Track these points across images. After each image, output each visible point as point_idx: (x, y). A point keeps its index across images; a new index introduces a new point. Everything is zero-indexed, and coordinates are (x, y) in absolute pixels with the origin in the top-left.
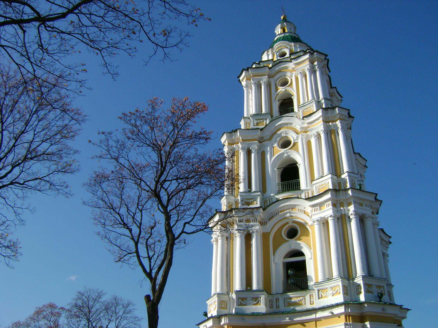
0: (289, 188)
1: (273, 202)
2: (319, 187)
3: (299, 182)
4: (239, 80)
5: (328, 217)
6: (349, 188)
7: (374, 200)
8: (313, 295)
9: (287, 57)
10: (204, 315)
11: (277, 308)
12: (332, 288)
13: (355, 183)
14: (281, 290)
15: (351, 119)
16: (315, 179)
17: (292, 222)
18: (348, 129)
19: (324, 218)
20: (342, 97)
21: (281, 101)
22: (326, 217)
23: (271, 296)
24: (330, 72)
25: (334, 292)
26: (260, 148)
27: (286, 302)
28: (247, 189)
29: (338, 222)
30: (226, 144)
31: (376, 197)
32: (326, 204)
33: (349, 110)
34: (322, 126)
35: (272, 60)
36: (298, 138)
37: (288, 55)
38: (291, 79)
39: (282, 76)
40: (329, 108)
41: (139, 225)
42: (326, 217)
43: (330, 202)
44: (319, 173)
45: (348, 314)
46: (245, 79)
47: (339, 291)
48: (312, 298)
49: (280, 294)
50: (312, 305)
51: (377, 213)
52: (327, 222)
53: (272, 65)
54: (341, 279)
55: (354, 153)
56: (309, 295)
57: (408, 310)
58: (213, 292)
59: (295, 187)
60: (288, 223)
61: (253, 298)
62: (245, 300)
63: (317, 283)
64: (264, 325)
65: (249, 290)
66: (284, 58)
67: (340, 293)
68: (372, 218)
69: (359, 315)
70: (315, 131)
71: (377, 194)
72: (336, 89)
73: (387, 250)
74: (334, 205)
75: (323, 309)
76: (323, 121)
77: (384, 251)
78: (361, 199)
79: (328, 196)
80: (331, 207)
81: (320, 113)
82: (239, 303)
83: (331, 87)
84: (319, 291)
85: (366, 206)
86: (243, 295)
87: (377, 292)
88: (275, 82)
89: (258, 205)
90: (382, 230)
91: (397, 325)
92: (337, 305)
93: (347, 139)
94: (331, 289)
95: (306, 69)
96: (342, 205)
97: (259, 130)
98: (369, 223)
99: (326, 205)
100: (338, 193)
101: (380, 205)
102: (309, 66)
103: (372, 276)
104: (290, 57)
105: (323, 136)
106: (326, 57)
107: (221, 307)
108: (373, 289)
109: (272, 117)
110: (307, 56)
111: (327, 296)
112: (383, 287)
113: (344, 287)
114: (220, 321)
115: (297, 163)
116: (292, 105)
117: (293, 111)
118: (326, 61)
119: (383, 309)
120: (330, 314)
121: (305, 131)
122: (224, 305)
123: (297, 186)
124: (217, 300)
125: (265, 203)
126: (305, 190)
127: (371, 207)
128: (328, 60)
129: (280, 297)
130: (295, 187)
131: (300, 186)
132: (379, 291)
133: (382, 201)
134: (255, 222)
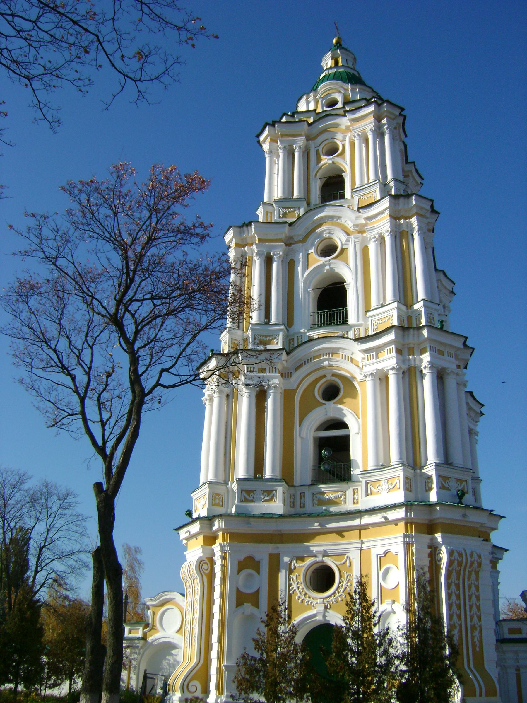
0: (330, 321)
1: (303, 341)
2: (377, 321)
3: (346, 312)
5: (388, 370)
6: (423, 327)
7: (461, 346)
8: (358, 489)
9: (339, 108)
10: (187, 515)
11: (300, 507)
12: (387, 480)
13: (433, 318)
14: (308, 479)
15: (435, 216)
16: (372, 309)
17: (331, 374)
18: (429, 230)
19: (382, 370)
20: (423, 179)
21: (324, 180)
22: (385, 369)
23: (292, 488)
24: (406, 136)
25: (391, 487)
26: (286, 254)
27: (316, 499)
28: (263, 320)
29: (403, 377)
30: (233, 245)
31: (465, 341)
32: (386, 349)
33: (432, 201)
34: (388, 225)
35: (315, 110)
36: (349, 241)
37: (340, 105)
38: (343, 145)
39: (328, 139)
40: (401, 196)
41: (87, 370)
42: (385, 369)
43: (393, 346)
44: (378, 299)
45: (410, 521)
46: (268, 140)
47: (398, 485)
48: (356, 494)
49: (307, 487)
51: (466, 368)
52: (387, 378)
53: (314, 119)
54: (402, 468)
55: (436, 270)
56: (351, 489)
57: (502, 517)
58: (202, 480)
59: (340, 319)
60: (325, 376)
61: (264, 491)
62: (252, 494)
63: (365, 472)
64: (279, 533)
65: (259, 478)
66: (333, 109)
67: (399, 488)
68: (457, 374)
69: (426, 522)
70: (376, 232)
71: (466, 338)
72: (415, 166)
73: (477, 425)
74: (399, 352)
75: (372, 511)
76: (391, 216)
77: (472, 427)
78: (441, 344)
79: (391, 336)
80: (394, 354)
81: (385, 203)
82: (243, 498)
83: (407, 162)
84: (367, 483)
85: (450, 355)
86: (249, 486)
87: (457, 489)
89: (280, 346)
90: (471, 393)
91: (482, 539)
92: (394, 506)
93: (426, 246)
94: (386, 481)
95: (368, 130)
96: (411, 351)
97: (287, 225)
98: (451, 383)
99: (386, 351)
100: (406, 332)
101: (471, 356)
102: (373, 124)
103: (450, 464)
104: (344, 107)
105: (388, 240)
106: (401, 111)
107: (214, 502)
108: (450, 484)
109: (308, 204)
110: (371, 108)
111: (380, 492)
112: (466, 481)
113: (407, 479)
114: (212, 525)
115: (346, 282)
116: (343, 187)
117: (342, 196)
118: (402, 118)
119: (464, 515)
120: (383, 520)
121: (361, 230)
122: (219, 501)
123: (343, 319)
124: (208, 493)
125: (290, 343)
126: (354, 326)
127: (457, 357)
128: (405, 117)
129: (306, 490)
130: (340, 319)
131: (346, 318)
132: (460, 488)
133: (473, 349)
134: (272, 372)
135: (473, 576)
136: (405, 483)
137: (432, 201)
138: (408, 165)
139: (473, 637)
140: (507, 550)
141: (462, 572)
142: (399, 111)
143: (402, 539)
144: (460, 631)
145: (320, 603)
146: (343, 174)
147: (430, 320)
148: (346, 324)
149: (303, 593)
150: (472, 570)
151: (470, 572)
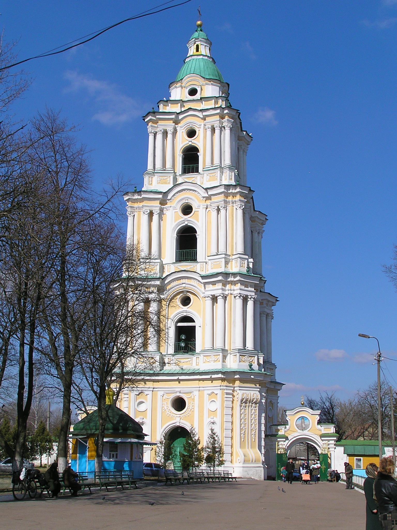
3: (196, 252)
4: (144, 120)
22: (216, 295)
26: (161, 210)
33: (250, 187)
37: (198, 96)
42: (216, 295)
47: (219, 359)
48: (198, 360)
74: (224, 285)
79: (220, 278)
83: (242, 130)
90: (269, 294)
100: (228, 275)
117: (197, 171)
123: (195, 256)
128: (240, 113)
137: (250, 187)
141: (248, 404)
146: (198, 153)
148: (196, 260)
150: (254, 403)
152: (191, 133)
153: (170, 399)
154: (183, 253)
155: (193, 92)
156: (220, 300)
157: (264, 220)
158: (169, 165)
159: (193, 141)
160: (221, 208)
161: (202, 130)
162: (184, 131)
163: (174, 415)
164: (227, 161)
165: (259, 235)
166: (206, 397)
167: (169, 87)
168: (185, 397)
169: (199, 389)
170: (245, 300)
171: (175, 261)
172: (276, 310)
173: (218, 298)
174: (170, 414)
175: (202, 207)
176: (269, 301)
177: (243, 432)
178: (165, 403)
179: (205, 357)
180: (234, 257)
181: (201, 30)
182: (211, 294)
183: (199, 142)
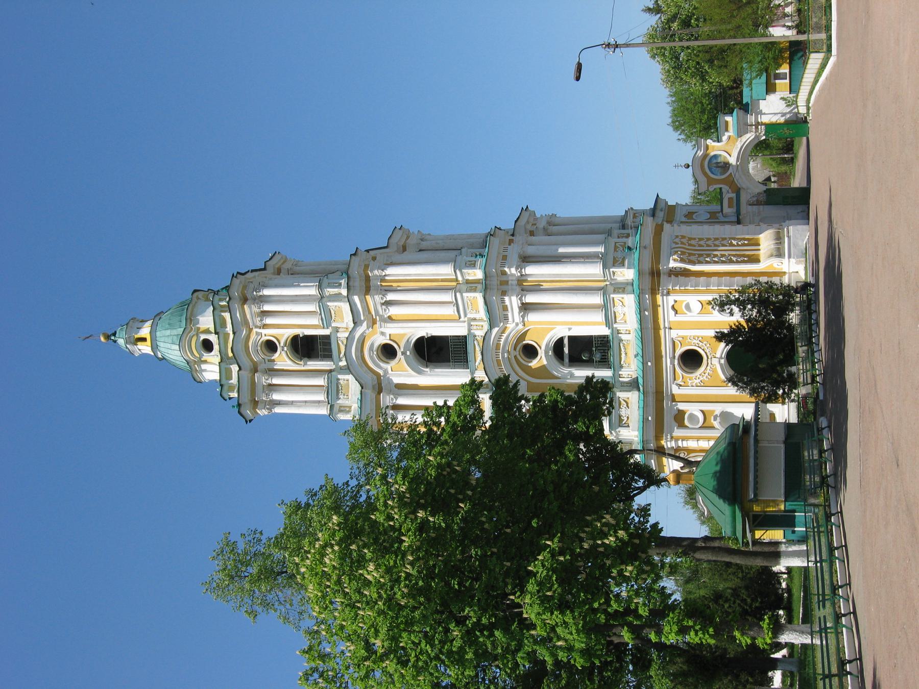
4: (250, 421)
26: (390, 392)
37: (213, 338)
42: (520, 305)
47: (620, 299)
50: (631, 332)
67: (623, 298)
83: (265, 269)
88: (267, 361)
90: (516, 222)
100: (488, 286)
112: (616, 243)
117: (328, 337)
118: (239, 275)
123: (459, 339)
126: (469, 330)
128: (238, 273)
131: (459, 336)
135: (693, 242)
136: (619, 293)
137: (351, 255)
138: (268, 268)
139: (738, 245)
140: (658, 195)
142: (234, 278)
143: (665, 297)
144: (734, 256)
145: (711, 361)
146: (301, 336)
147: (472, 264)
148: (466, 337)
149: (703, 374)
151: (690, 245)
152: (271, 346)
153: (684, 374)
154: (455, 357)
155: (207, 346)
156: (530, 298)
157: (401, 232)
158: (321, 381)
159: (282, 344)
160: (385, 299)
161: (264, 331)
162: (266, 358)
163: (709, 368)
164: (311, 290)
165: (426, 240)
166: (679, 318)
167: (200, 382)
168: (679, 351)
169: (667, 330)
170: (526, 260)
171: (469, 370)
172: (541, 210)
173: (524, 302)
174: (707, 374)
175: (383, 330)
176: (528, 222)
177: (734, 259)
178: (690, 382)
179: (617, 321)
180: (460, 278)
181: (114, 334)
182: (518, 314)
183: (283, 335)
